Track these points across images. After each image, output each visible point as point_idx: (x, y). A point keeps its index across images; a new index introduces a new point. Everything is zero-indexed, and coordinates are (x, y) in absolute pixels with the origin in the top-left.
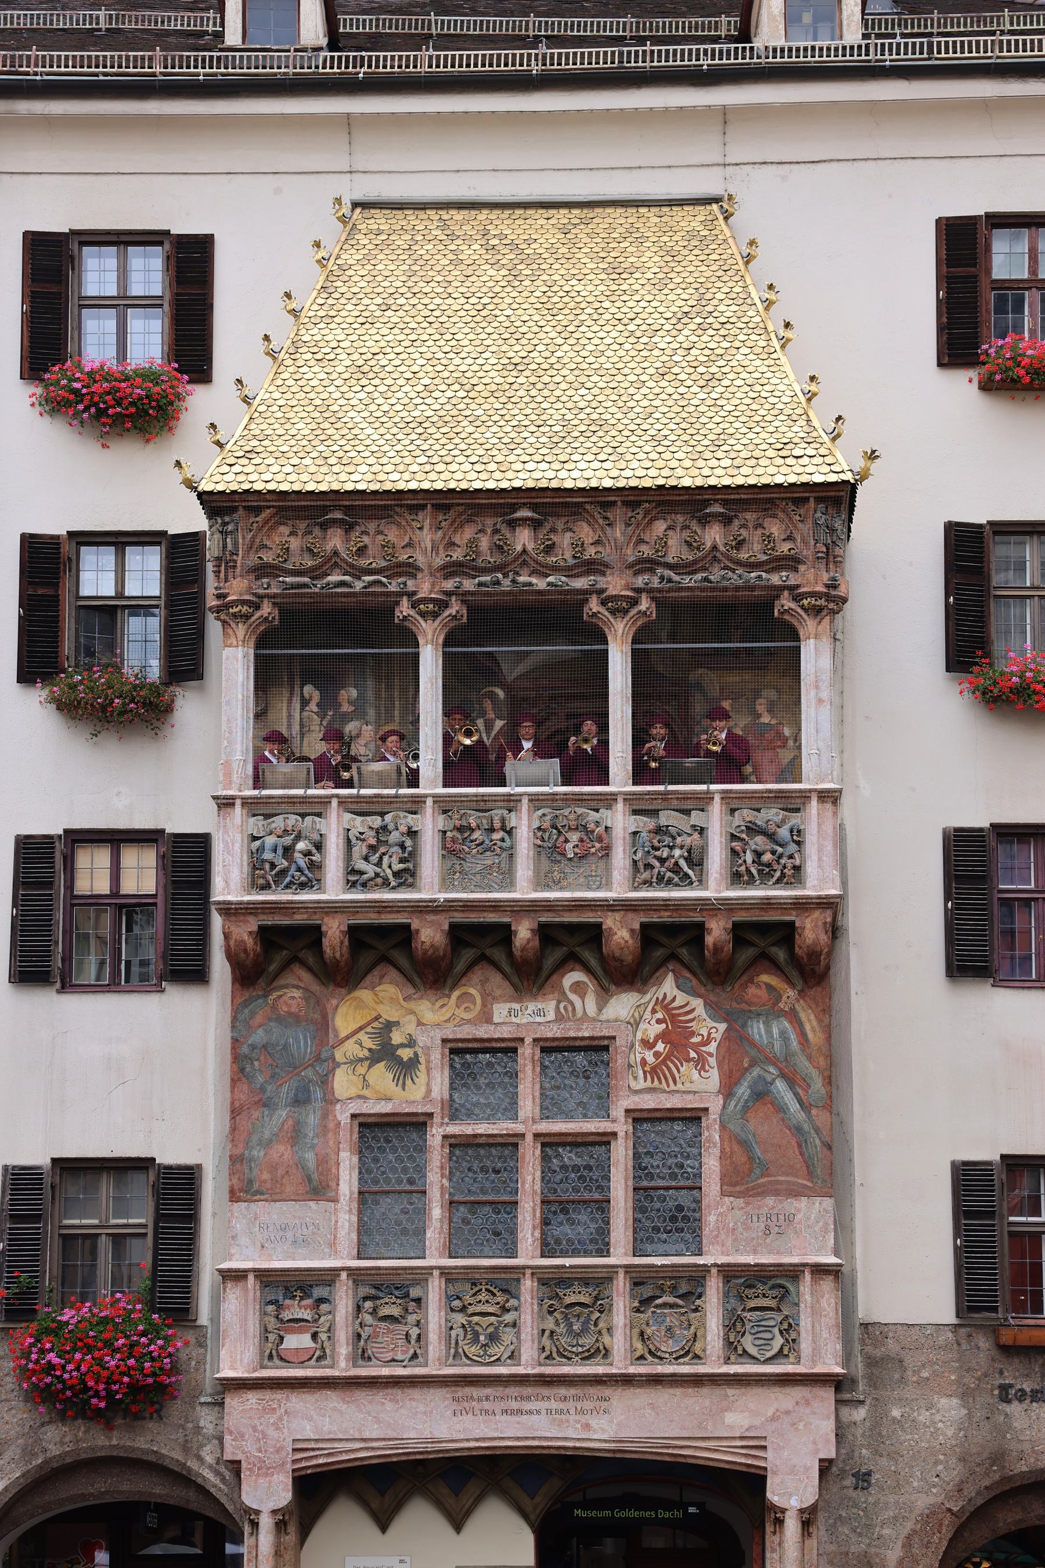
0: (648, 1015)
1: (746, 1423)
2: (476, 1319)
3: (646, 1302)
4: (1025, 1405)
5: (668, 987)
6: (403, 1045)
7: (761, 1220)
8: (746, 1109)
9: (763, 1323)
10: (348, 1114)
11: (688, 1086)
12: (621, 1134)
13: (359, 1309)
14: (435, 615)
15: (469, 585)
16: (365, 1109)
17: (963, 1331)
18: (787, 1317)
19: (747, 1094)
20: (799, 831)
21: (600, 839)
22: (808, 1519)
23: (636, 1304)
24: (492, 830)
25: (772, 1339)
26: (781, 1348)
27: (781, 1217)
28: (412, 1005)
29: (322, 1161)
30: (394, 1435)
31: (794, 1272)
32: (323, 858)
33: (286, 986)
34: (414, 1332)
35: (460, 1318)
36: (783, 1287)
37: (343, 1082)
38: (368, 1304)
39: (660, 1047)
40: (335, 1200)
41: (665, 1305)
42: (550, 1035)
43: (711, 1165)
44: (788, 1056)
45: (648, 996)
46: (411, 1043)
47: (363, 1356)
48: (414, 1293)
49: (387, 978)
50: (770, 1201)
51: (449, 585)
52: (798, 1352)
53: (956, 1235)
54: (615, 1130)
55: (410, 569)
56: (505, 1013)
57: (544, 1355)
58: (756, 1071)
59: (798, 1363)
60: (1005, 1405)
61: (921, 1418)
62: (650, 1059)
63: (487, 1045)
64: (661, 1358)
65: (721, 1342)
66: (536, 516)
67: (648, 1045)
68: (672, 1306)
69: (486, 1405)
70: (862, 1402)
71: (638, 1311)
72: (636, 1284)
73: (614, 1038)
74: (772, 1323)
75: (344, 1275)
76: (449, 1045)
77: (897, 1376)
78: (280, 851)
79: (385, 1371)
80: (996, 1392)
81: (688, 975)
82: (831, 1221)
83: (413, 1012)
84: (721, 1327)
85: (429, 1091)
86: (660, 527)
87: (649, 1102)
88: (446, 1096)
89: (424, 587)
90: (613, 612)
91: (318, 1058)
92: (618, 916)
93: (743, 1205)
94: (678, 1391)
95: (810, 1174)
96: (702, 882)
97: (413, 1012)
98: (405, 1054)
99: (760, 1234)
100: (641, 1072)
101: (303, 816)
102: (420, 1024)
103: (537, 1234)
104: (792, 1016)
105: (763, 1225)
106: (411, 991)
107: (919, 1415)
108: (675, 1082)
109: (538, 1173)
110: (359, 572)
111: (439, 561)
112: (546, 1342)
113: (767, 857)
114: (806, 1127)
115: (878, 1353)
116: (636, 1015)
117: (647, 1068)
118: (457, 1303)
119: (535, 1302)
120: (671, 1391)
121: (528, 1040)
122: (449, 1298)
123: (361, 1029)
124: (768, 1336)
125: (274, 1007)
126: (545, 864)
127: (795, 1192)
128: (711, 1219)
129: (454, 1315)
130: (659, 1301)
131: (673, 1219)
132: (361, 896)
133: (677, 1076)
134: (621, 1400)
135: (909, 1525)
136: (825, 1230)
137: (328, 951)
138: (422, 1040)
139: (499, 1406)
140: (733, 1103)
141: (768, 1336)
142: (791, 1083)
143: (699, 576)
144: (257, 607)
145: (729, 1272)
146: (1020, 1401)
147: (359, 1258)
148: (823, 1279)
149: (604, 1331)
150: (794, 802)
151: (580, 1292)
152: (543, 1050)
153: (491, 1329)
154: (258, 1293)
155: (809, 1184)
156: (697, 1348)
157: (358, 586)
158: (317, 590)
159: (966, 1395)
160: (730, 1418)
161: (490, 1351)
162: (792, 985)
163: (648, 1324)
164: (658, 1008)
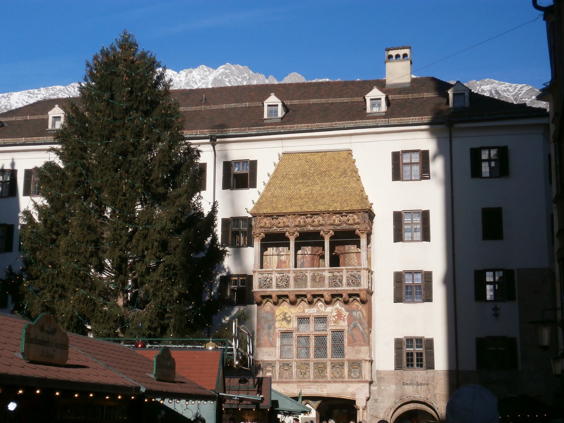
1: (352, 390)
2: (301, 370)
5: (338, 305)
6: (288, 317)
8: (352, 329)
11: (341, 325)
12: (329, 334)
13: (280, 368)
14: (292, 235)
15: (299, 229)
16: (281, 329)
21: (323, 278)
22: (365, 408)
24: (303, 276)
28: (290, 309)
29: (273, 339)
30: (286, 392)
31: (361, 361)
32: (272, 282)
34: (290, 373)
37: (277, 325)
38: (282, 367)
39: (336, 317)
40: (276, 347)
42: (315, 315)
43: (346, 340)
44: (360, 319)
46: (290, 317)
47: (280, 377)
48: (290, 365)
50: (357, 347)
51: (295, 229)
53: (395, 353)
55: (288, 226)
58: (354, 322)
62: (334, 320)
66: (311, 216)
67: (334, 317)
68: (339, 368)
69: (304, 387)
70: (376, 386)
71: (332, 368)
75: (277, 361)
77: (383, 381)
78: (264, 281)
79: (285, 380)
82: (368, 350)
83: (290, 311)
85: (293, 326)
86: (334, 217)
87: (334, 328)
88: (296, 327)
89: (291, 231)
90: (325, 234)
91: (273, 320)
92: (326, 292)
95: (365, 342)
96: (342, 286)
97: (290, 311)
98: (289, 319)
101: (269, 274)
102: (291, 313)
103: (313, 353)
104: (361, 311)
109: (313, 342)
110: (279, 227)
111: (293, 225)
112: (314, 375)
113: (354, 281)
115: (380, 376)
118: (298, 367)
121: (312, 316)
122: (297, 366)
123: (280, 314)
125: (265, 310)
126: (313, 282)
127: (362, 345)
128: (346, 351)
129: (298, 369)
131: (340, 351)
132: (279, 290)
134: (328, 385)
135: (385, 410)
138: (292, 316)
139: (306, 387)
142: (361, 324)
143: (342, 226)
144: (260, 234)
145: (349, 361)
147: (280, 358)
150: (359, 270)
152: (315, 318)
153: (304, 372)
156: (343, 376)
157: (278, 231)
158: (271, 231)
159: (396, 384)
160: (349, 389)
161: (304, 376)
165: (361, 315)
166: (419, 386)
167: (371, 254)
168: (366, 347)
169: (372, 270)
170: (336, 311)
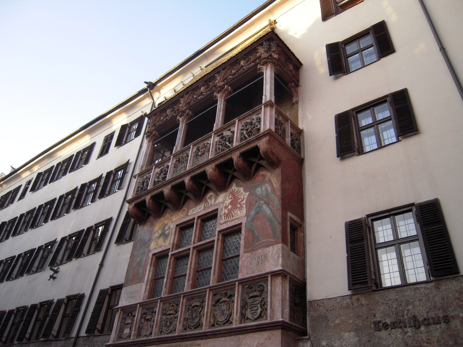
0: (227, 198)
3: (218, 301)
4: (388, 332)
5: (234, 187)
7: (256, 259)
8: (253, 219)
9: (254, 303)
10: (152, 254)
11: (237, 217)
17: (355, 297)
18: (263, 298)
19: (254, 213)
20: (260, 119)
23: (214, 303)
25: (257, 310)
26: (261, 314)
27: (263, 256)
33: (147, 223)
35: (164, 317)
36: (262, 286)
41: (223, 302)
43: (242, 242)
44: (267, 195)
45: (228, 192)
49: (168, 212)
50: (259, 251)
52: (266, 314)
53: (347, 252)
54: (214, 239)
56: (192, 212)
57: (184, 328)
58: (257, 204)
59: (267, 319)
60: (378, 332)
61: (336, 345)
63: (188, 223)
64: (219, 324)
65: (239, 314)
67: (226, 207)
71: (215, 306)
72: (215, 295)
73: (217, 210)
74: (257, 302)
76: (179, 227)
77: (324, 324)
80: (372, 326)
81: (239, 181)
84: (239, 308)
87: (224, 226)
93: (250, 255)
94: (222, 339)
99: (255, 265)
100: (223, 217)
104: (270, 181)
105: (256, 261)
106: (172, 213)
107: (335, 343)
108: (233, 217)
114: (273, 219)
116: (224, 199)
117: (225, 215)
119: (184, 307)
120: (221, 339)
124: (256, 308)
130: (221, 301)
133: (233, 215)
136: (278, 257)
137: (147, 206)
140: (250, 218)
141: (256, 308)
142: (268, 204)
145: (243, 282)
146: (386, 330)
148: (277, 279)
149: (202, 316)
151: (197, 301)
154: (121, 316)
155: (273, 240)
159: (357, 330)
162: (269, 171)
163: (216, 311)
164: (230, 195)
165: (269, 189)
166: (422, 328)
167: (298, 110)
168: (276, 245)
169: (300, 127)
170: (230, 197)
